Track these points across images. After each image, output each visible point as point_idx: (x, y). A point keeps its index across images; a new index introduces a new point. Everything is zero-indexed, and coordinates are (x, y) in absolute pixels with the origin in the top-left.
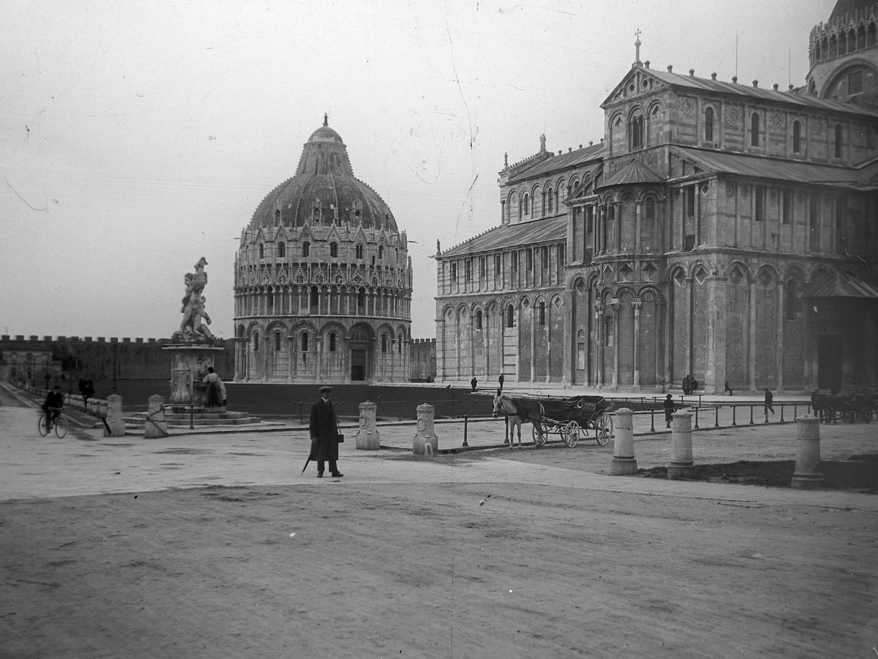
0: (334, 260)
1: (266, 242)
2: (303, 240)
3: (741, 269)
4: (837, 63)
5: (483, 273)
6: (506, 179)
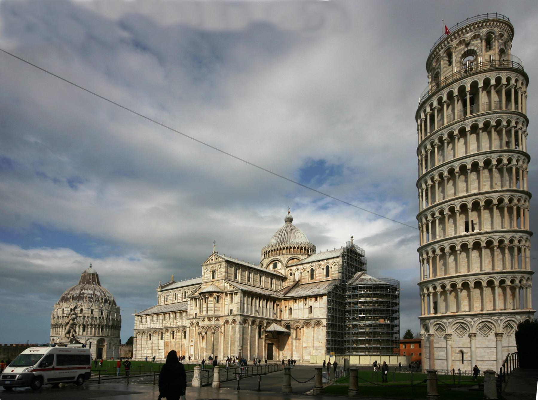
4: (270, 259)
5: (152, 321)
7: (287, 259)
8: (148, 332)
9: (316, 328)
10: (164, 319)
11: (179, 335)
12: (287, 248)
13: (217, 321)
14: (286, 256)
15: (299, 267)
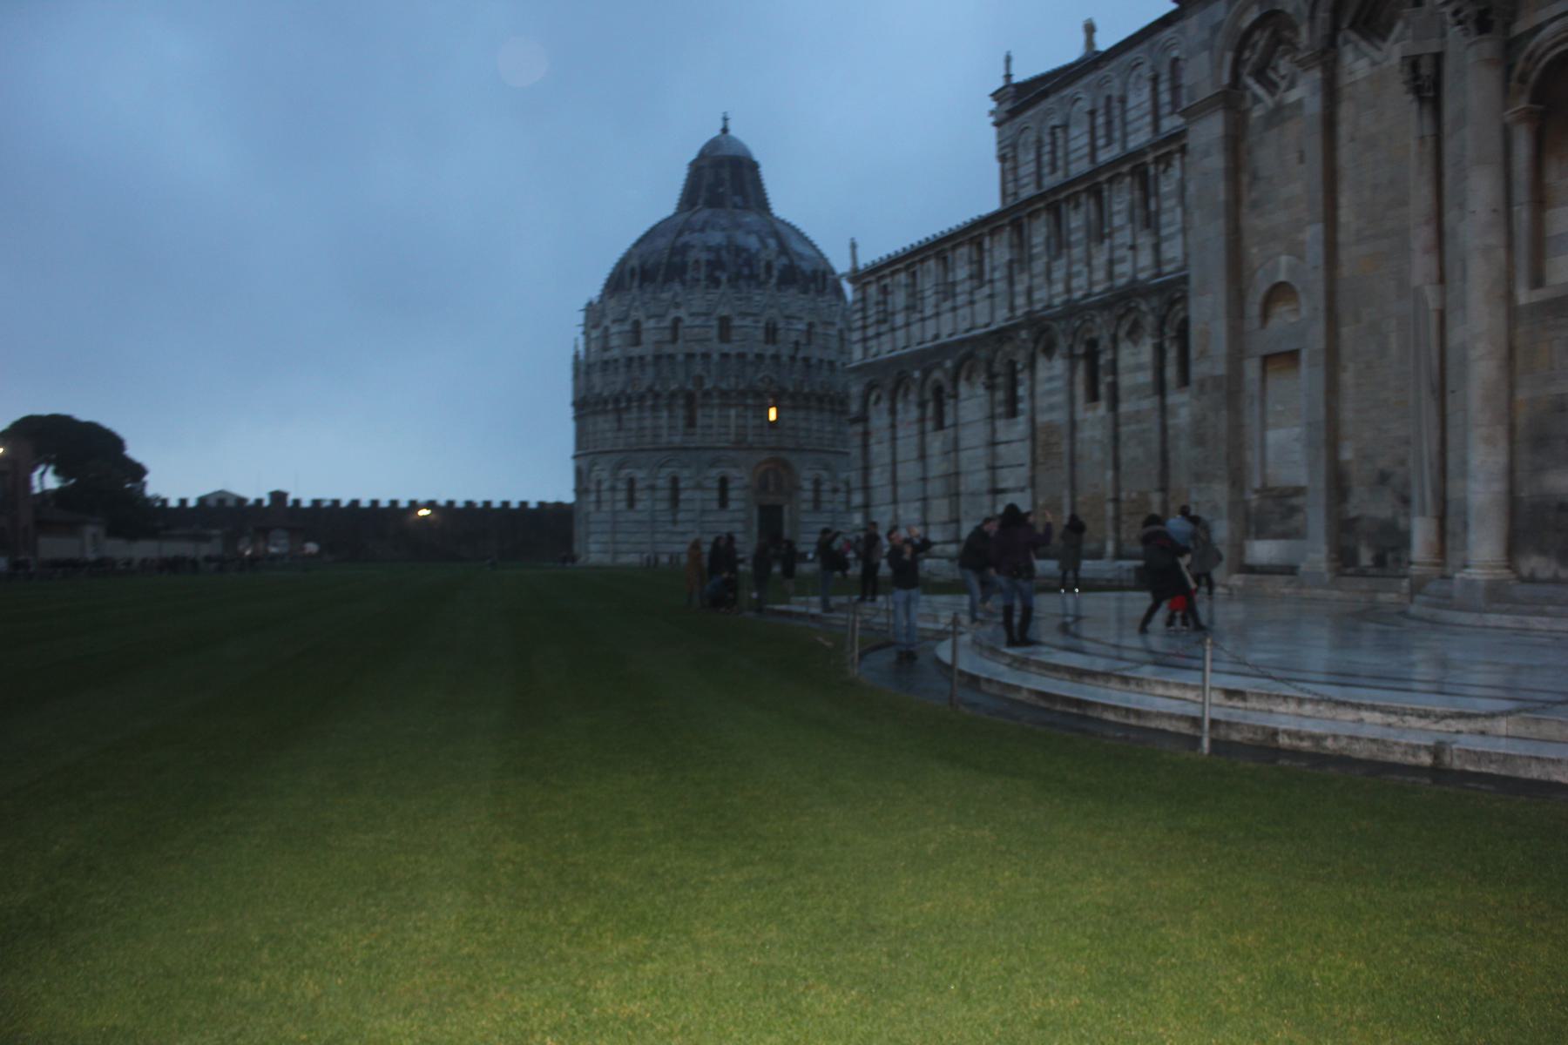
0: (726, 348)
1: (614, 321)
2: (673, 313)
5: (947, 290)
6: (1008, 106)
8: (926, 373)
10: (1020, 261)
11: (1135, 360)
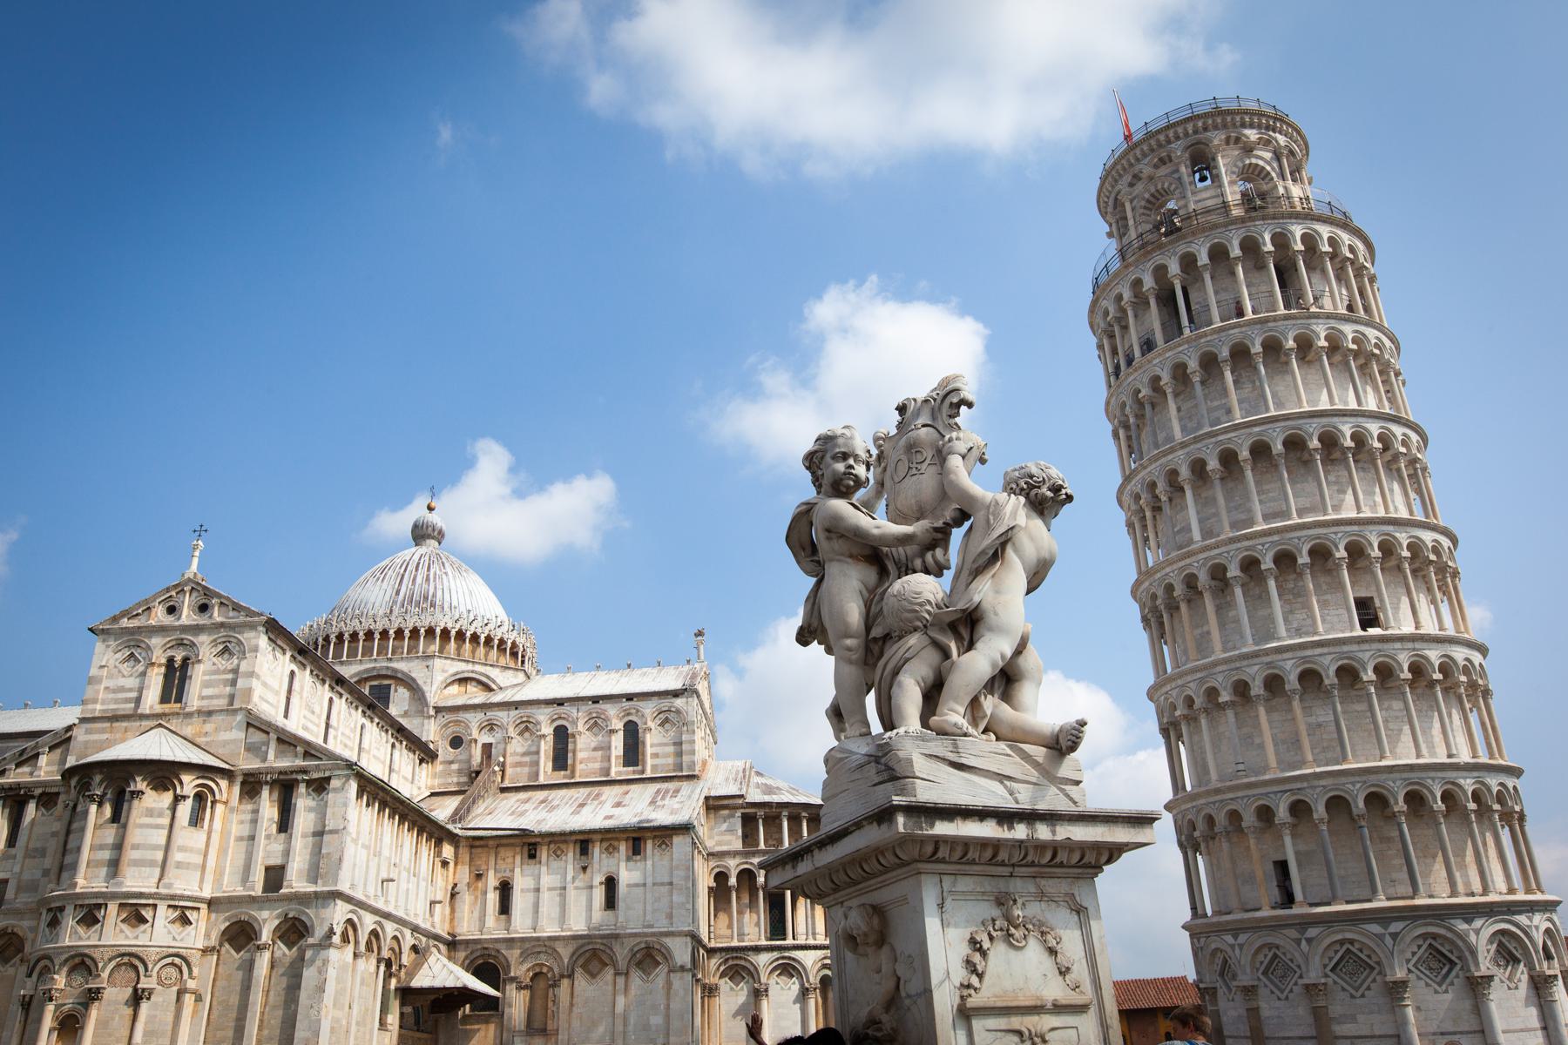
3: (351, 933)
7: (439, 678)
9: (636, 979)
12: (445, 633)
13: (177, 927)
14: (438, 663)
15: (502, 716)
